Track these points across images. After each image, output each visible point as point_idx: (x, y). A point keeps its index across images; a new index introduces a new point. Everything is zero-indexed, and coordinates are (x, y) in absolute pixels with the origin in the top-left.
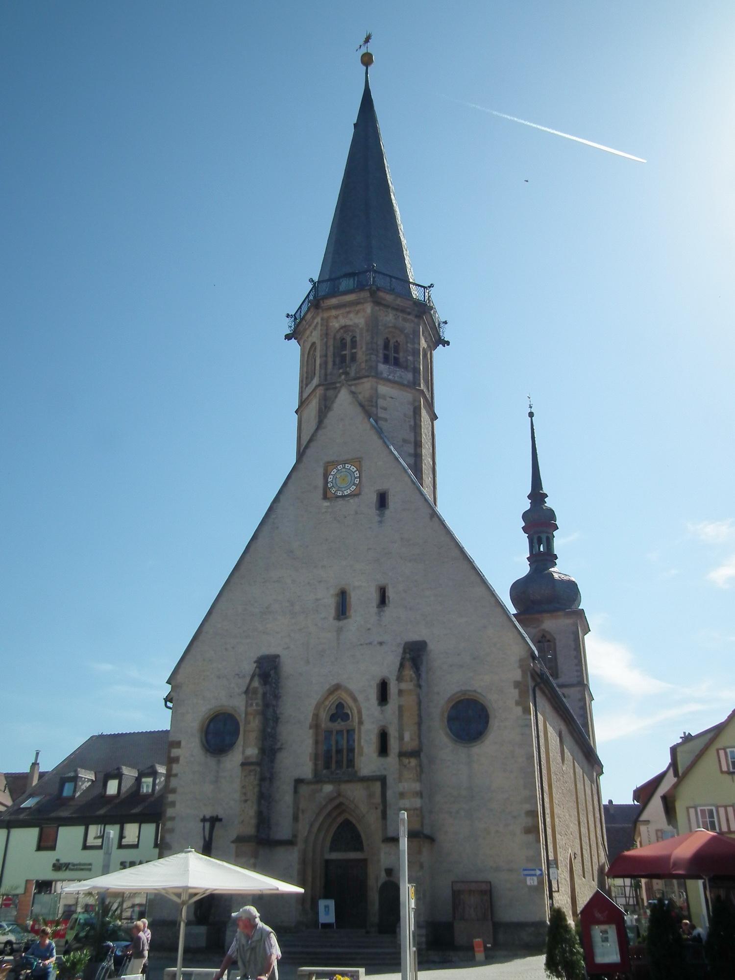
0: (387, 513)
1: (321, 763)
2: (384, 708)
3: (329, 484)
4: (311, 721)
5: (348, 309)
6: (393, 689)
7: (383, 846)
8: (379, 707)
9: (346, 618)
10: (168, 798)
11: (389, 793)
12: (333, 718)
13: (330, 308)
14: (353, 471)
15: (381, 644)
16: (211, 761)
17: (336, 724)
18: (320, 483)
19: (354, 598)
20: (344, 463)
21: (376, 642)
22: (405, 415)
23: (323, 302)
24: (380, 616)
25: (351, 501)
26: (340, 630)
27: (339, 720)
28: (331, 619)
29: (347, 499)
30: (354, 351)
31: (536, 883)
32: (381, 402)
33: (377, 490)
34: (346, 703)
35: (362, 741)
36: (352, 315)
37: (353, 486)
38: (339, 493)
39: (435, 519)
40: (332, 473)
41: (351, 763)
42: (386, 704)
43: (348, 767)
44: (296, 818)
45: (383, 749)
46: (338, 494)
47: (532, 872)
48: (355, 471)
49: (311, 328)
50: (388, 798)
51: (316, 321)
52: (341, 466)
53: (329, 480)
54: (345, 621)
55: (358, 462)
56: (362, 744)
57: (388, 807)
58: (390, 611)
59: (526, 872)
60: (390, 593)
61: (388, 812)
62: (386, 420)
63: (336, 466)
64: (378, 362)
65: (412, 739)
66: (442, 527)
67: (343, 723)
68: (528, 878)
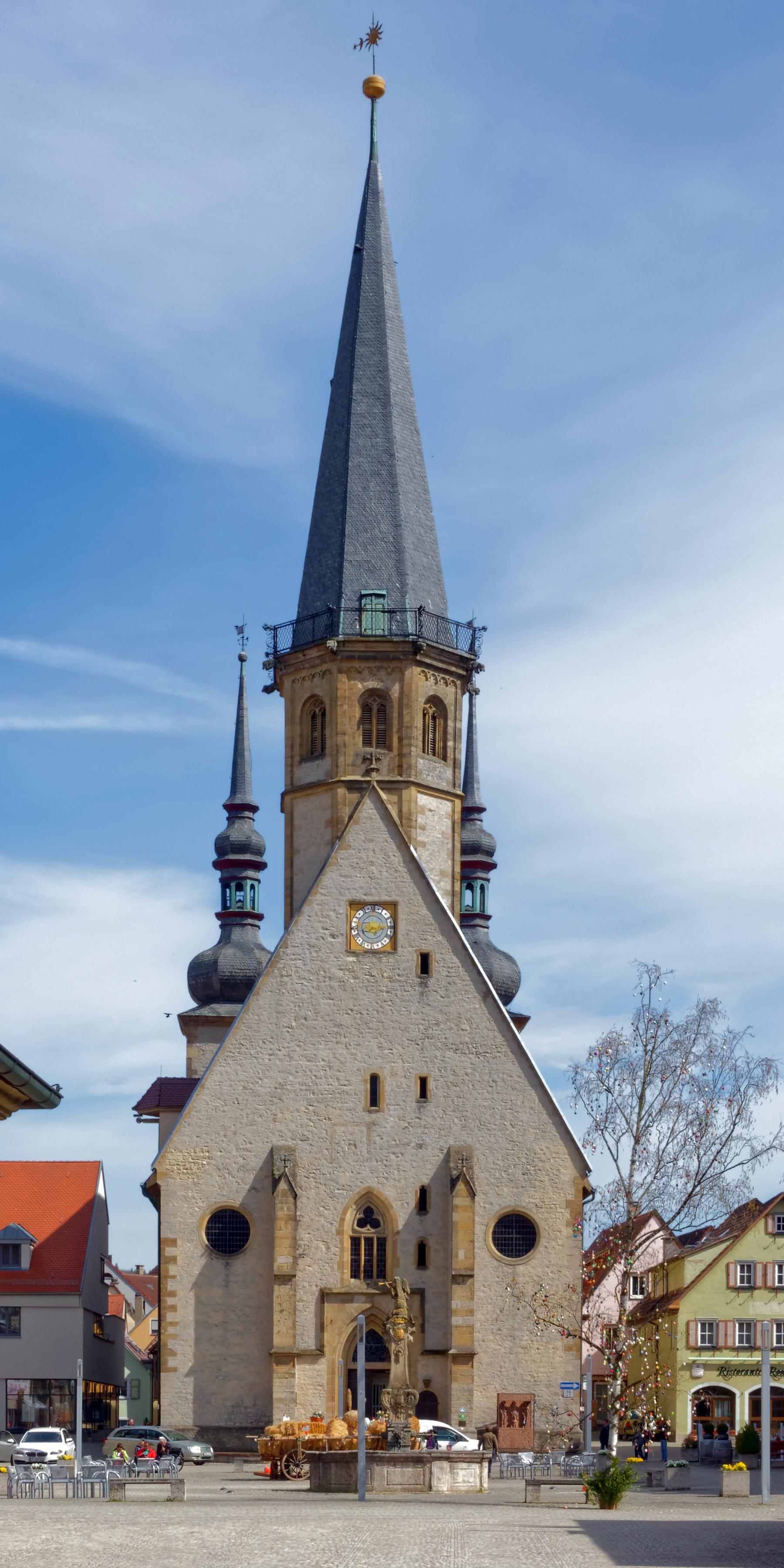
0: (432, 982)
1: (347, 1272)
2: (423, 1218)
3: (353, 931)
4: (337, 1226)
5: (378, 664)
6: (433, 1199)
7: (420, 1358)
8: (418, 1217)
9: (377, 1111)
10: (166, 1302)
11: (428, 1307)
12: (361, 1223)
13: (350, 658)
14: (386, 917)
15: (420, 1146)
16: (219, 1264)
17: (364, 1230)
18: (343, 928)
19: (387, 1087)
20: (374, 904)
21: (413, 1145)
22: (443, 833)
23: (344, 645)
24: (420, 1113)
25: (384, 959)
26: (371, 1125)
27: (368, 1227)
28: (360, 1109)
29: (378, 956)
30: (382, 727)
31: (572, 1395)
32: (421, 820)
33: (416, 951)
34: (378, 1209)
35: (398, 1252)
36: (382, 673)
37: (385, 939)
38: (367, 946)
39: (490, 1000)
40: (357, 915)
41: (382, 1275)
42: (426, 1214)
43: (378, 1277)
44: (321, 1328)
45: (422, 1261)
46: (366, 946)
47: (570, 1386)
48: (388, 918)
49: (313, 671)
50: (426, 1312)
51: (324, 667)
52: (369, 907)
53: (354, 925)
54: (378, 1115)
55: (392, 906)
56: (399, 1254)
57: (426, 1320)
58: (431, 1107)
59: (563, 1386)
60: (431, 1085)
61: (426, 1325)
62: (423, 844)
63: (362, 906)
64: (418, 756)
65: (466, 1257)
66: (498, 1011)
67: (373, 1230)
68: (565, 1391)
